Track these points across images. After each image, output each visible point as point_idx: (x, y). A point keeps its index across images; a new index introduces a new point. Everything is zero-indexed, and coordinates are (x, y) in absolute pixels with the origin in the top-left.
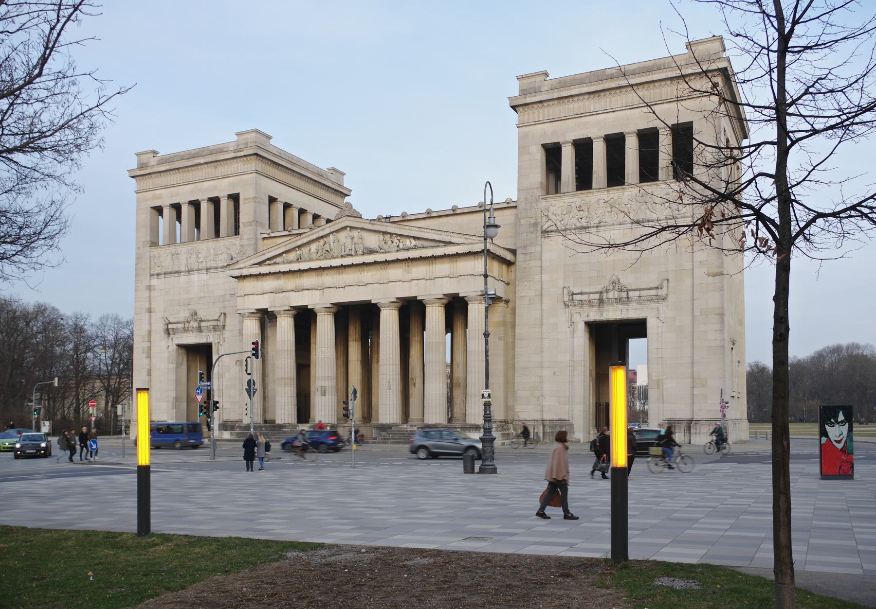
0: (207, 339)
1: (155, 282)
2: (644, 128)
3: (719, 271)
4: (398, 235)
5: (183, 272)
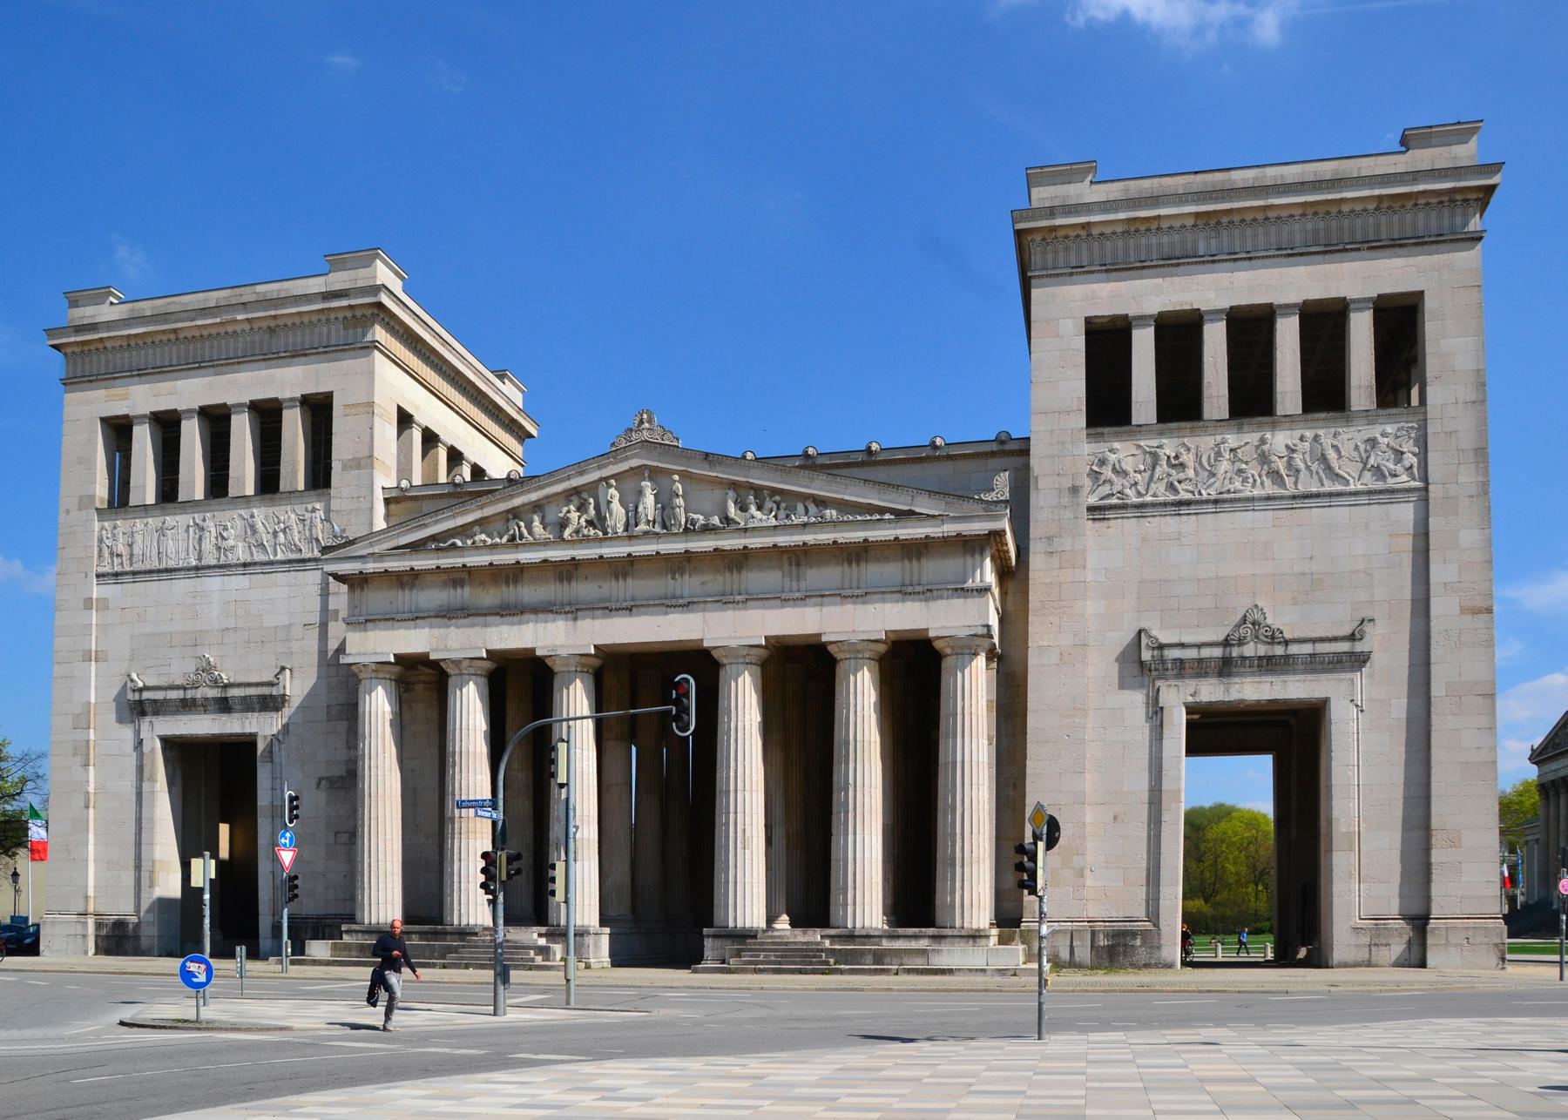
1: (111, 591)
2: (1317, 297)
3: (1485, 604)
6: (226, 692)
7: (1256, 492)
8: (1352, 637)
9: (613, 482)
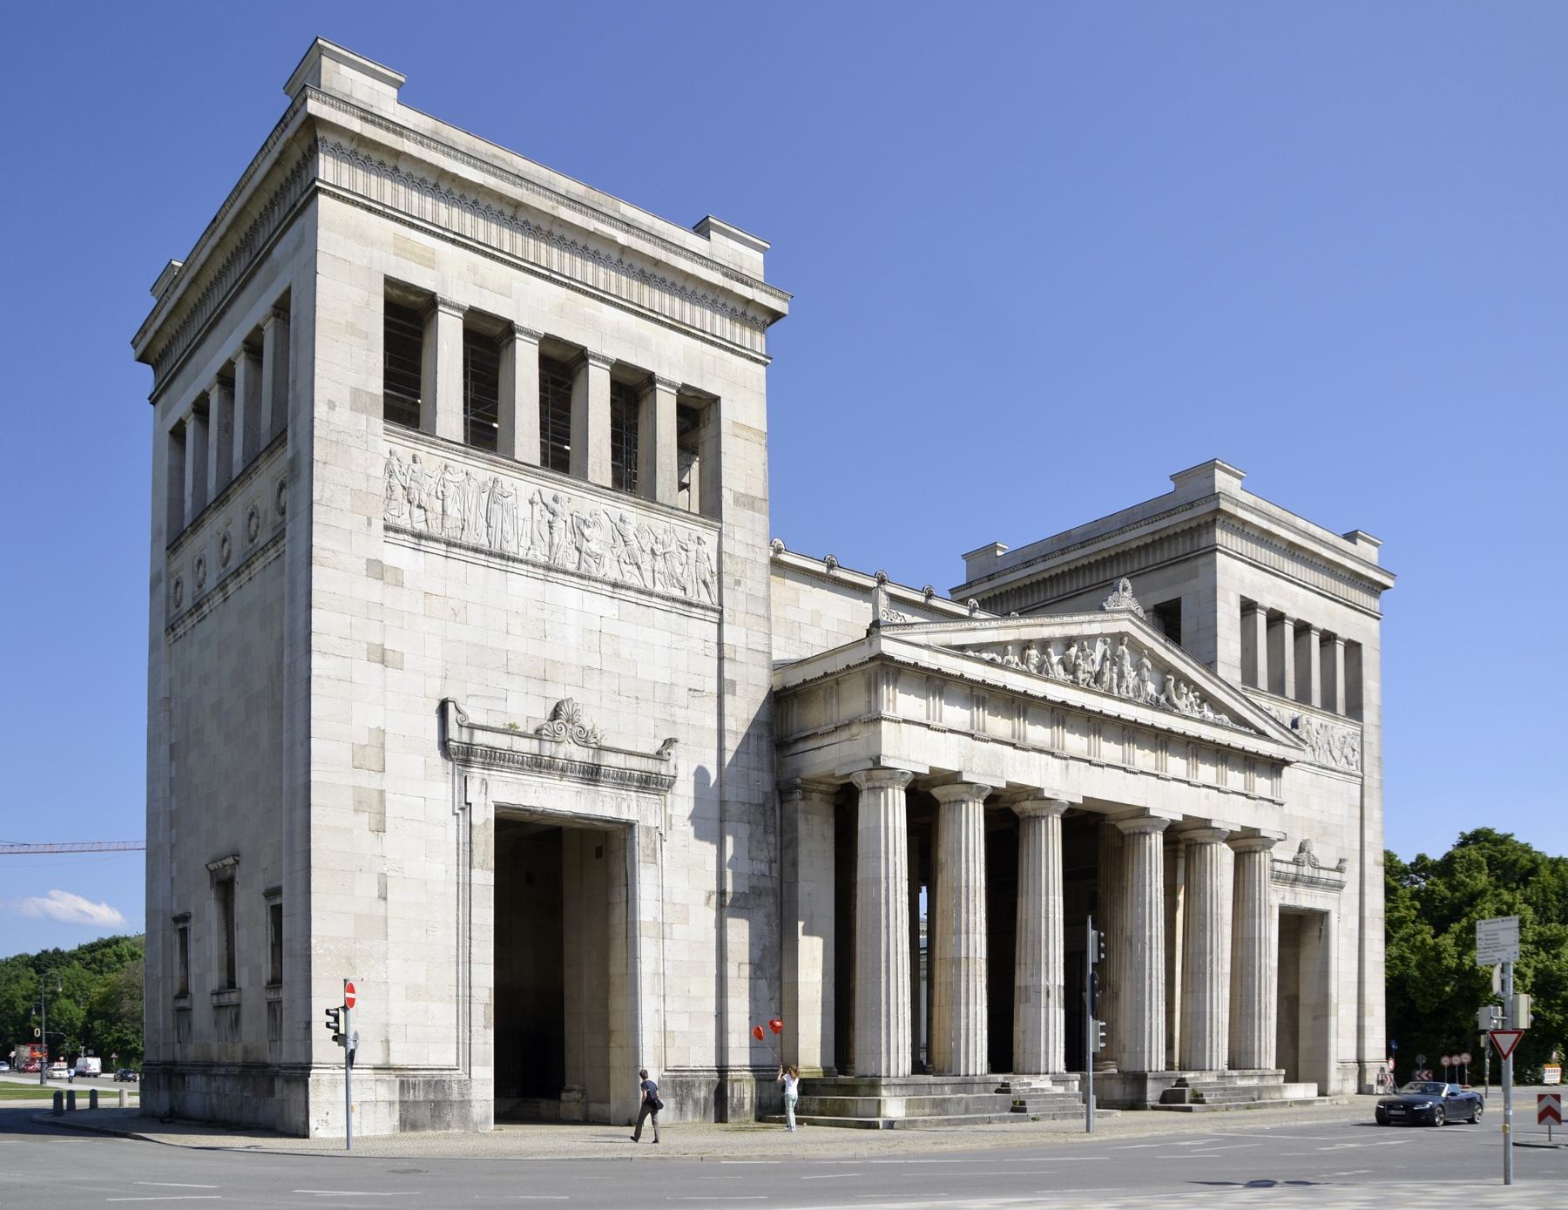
0: (619, 808)
5: (527, 563)
6: (599, 758)
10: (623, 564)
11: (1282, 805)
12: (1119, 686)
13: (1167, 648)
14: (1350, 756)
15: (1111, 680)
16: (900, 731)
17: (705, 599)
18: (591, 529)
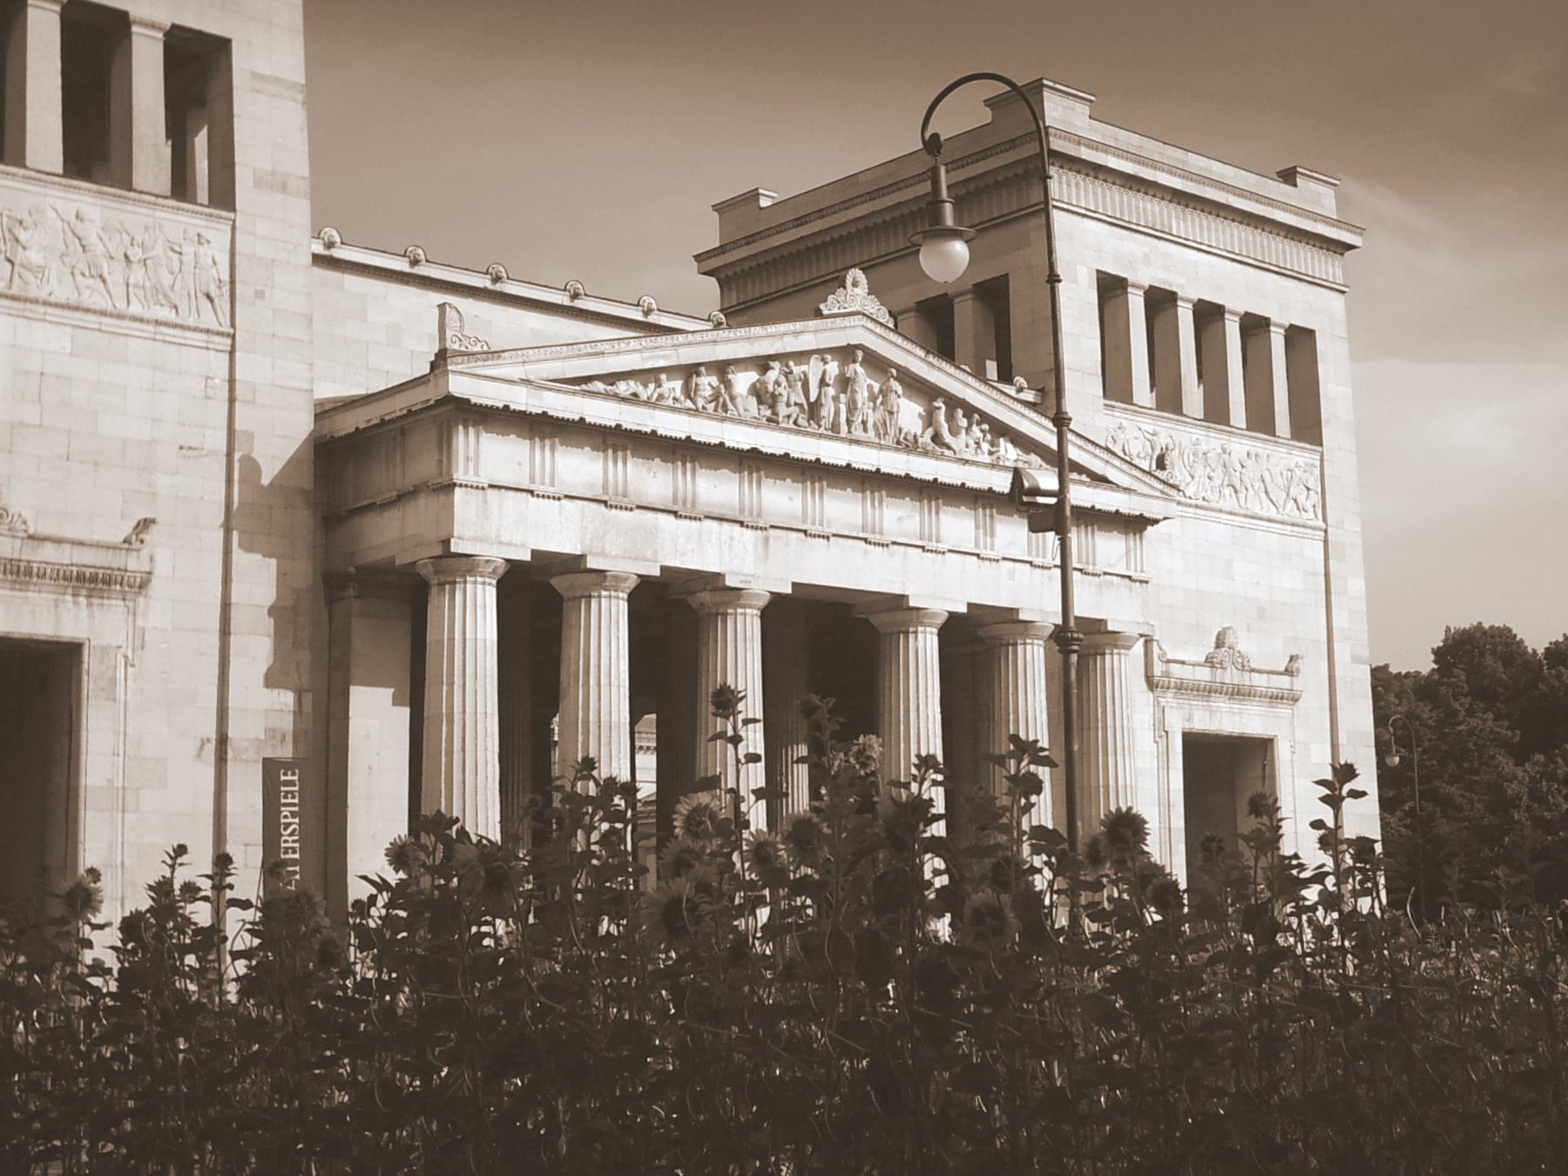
4: (985, 417)
7: (1222, 505)
8: (1288, 672)
9: (829, 357)
10: (79, 278)
11: (1147, 582)
12: (849, 422)
13: (930, 363)
14: (1302, 499)
15: (837, 413)
16: (486, 502)
17: (208, 320)
18: (30, 232)
